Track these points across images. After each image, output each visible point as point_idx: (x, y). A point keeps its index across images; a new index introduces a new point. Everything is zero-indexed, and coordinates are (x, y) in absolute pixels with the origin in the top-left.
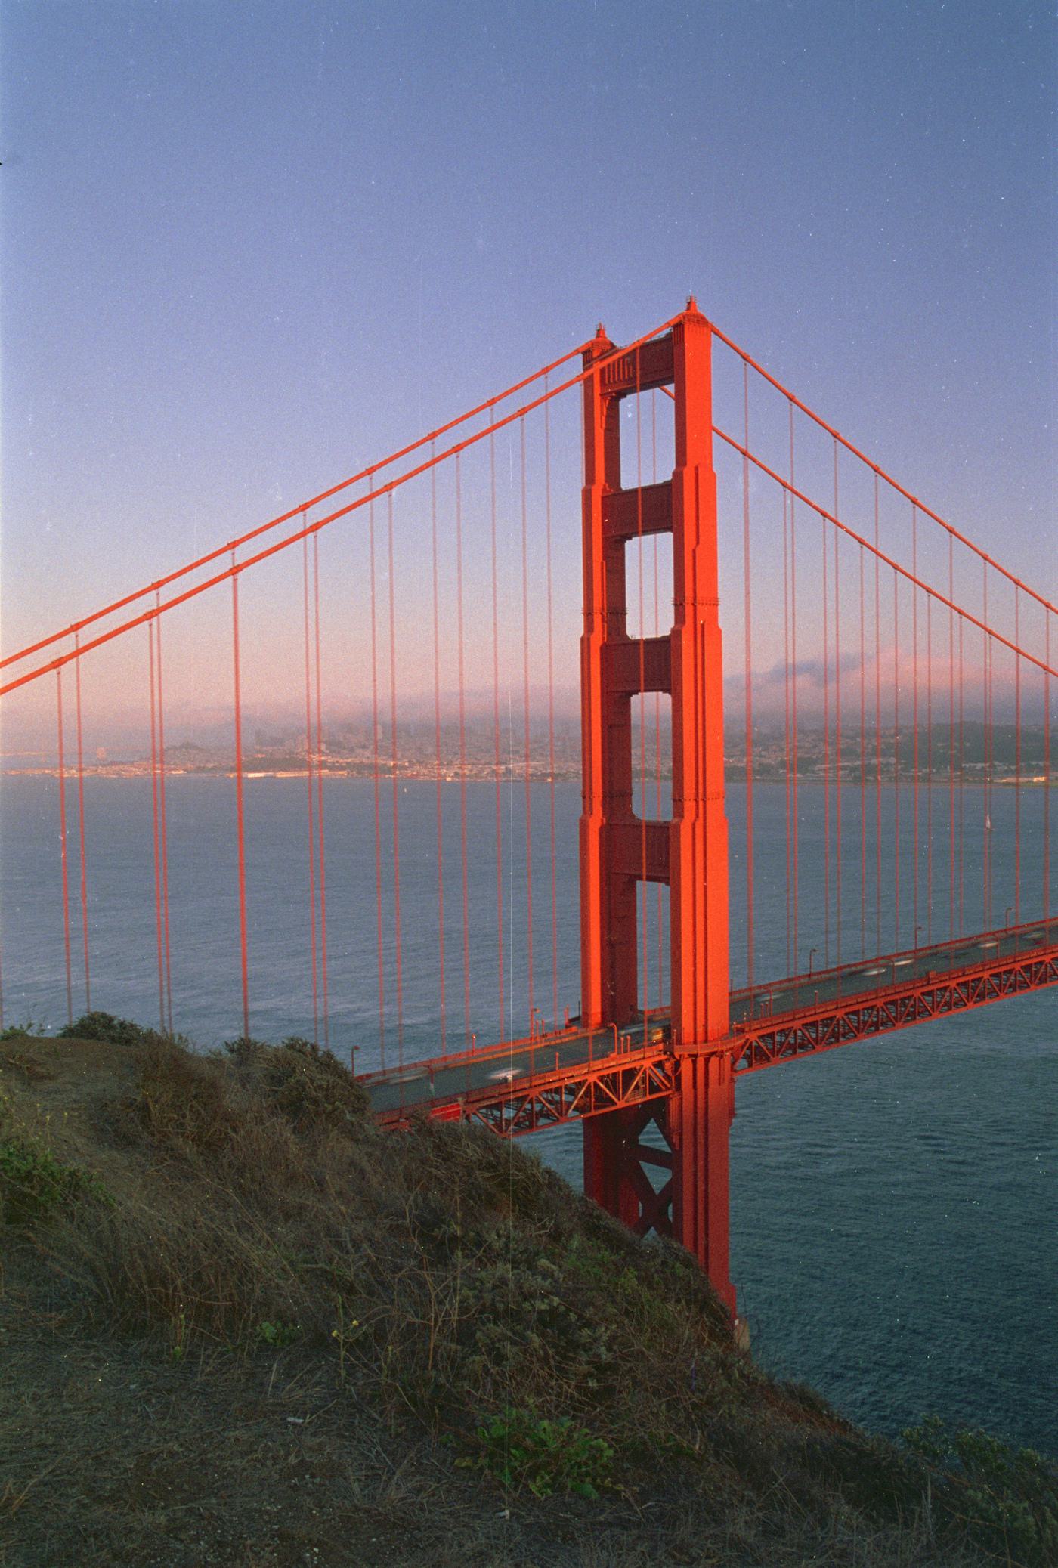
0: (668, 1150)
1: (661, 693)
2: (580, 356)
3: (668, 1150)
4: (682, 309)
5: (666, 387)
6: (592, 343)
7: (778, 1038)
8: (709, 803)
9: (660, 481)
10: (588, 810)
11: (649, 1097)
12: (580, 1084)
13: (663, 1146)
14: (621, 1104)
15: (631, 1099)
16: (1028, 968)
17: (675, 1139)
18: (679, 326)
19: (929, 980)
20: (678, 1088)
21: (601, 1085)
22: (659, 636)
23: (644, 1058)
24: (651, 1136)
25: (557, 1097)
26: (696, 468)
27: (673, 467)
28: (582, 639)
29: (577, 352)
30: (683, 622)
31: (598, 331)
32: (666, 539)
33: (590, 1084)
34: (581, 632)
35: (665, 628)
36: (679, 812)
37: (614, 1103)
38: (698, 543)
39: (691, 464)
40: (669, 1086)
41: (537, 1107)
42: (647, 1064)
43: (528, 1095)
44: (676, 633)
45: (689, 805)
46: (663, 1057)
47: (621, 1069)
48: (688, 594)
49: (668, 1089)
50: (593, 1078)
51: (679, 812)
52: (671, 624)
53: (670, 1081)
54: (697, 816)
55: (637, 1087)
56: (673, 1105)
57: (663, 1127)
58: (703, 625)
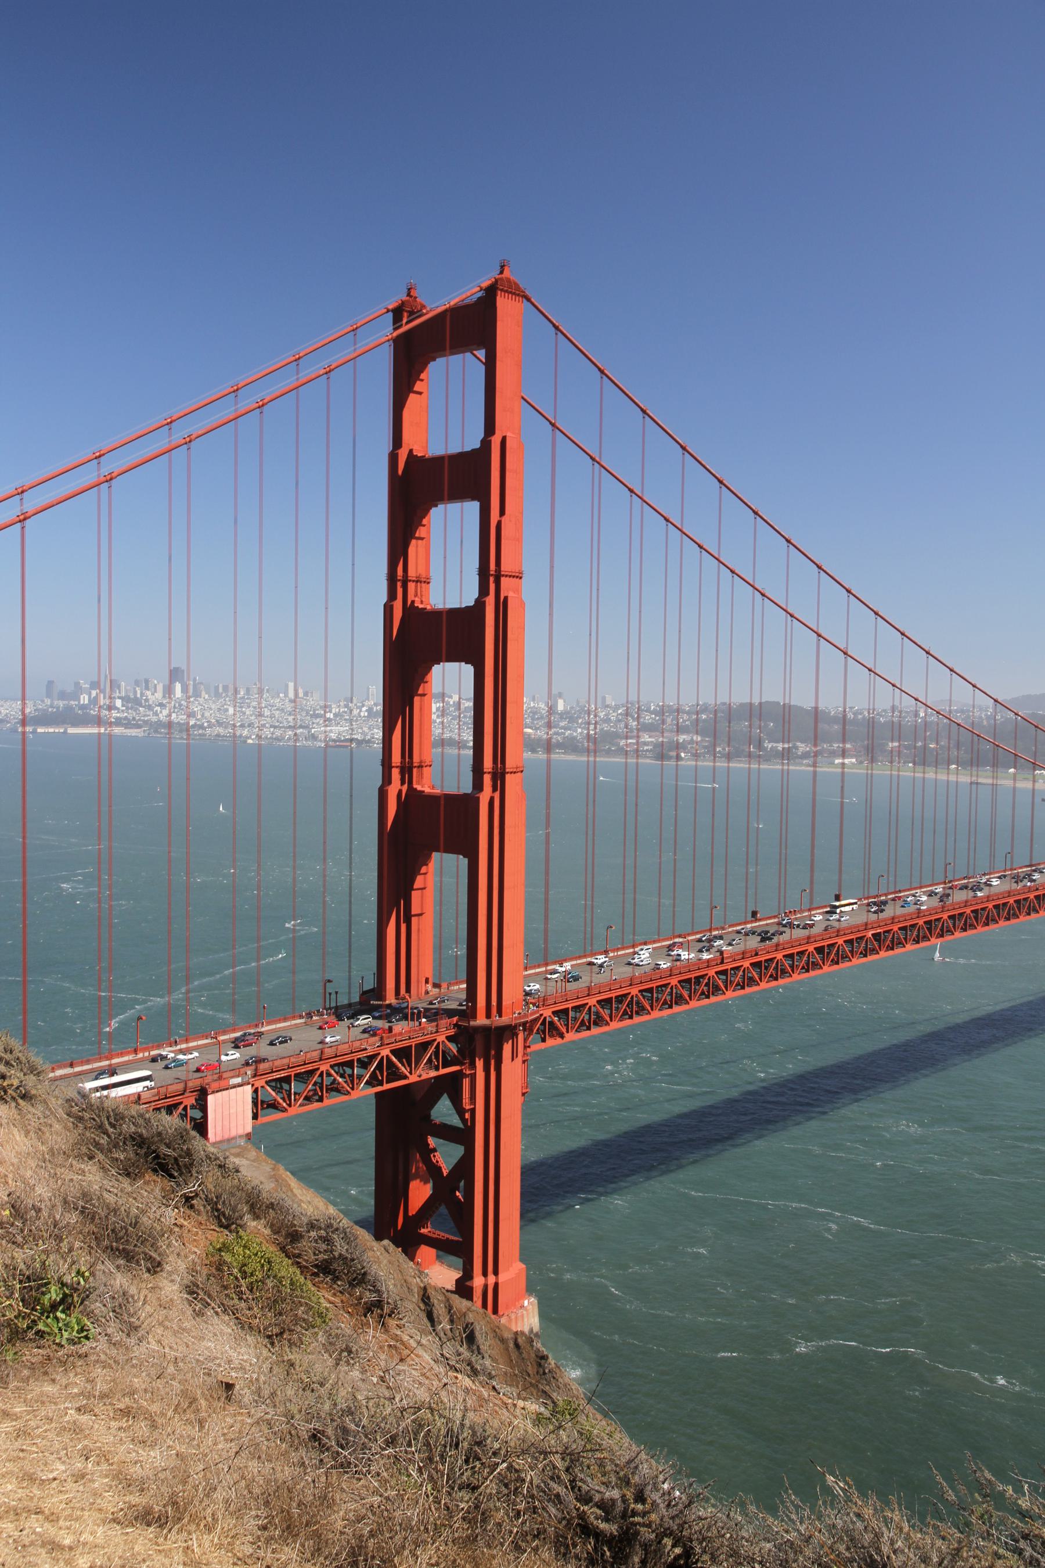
0: (461, 1126)
1: (463, 664)
2: (390, 315)
3: (461, 1126)
4: (494, 274)
5: (475, 352)
6: (403, 303)
7: (571, 1014)
8: (508, 776)
9: (468, 449)
10: (387, 779)
11: (443, 1071)
12: (372, 1058)
14: (413, 1079)
15: (422, 1073)
16: (820, 950)
18: (491, 292)
19: (723, 959)
21: (394, 1059)
22: (463, 606)
23: (437, 1032)
24: (443, 1111)
25: (348, 1071)
26: (504, 442)
27: (481, 435)
28: (385, 605)
30: (487, 594)
31: (409, 289)
32: (473, 507)
33: (383, 1057)
34: (384, 599)
35: (469, 599)
36: (478, 785)
37: (405, 1077)
38: (502, 512)
41: (327, 1081)
42: (441, 1038)
44: (480, 604)
45: (487, 779)
47: (413, 1043)
50: (385, 1052)
51: (478, 785)
52: (476, 595)
54: (494, 790)
55: (430, 1061)
57: (456, 1102)
58: (506, 598)
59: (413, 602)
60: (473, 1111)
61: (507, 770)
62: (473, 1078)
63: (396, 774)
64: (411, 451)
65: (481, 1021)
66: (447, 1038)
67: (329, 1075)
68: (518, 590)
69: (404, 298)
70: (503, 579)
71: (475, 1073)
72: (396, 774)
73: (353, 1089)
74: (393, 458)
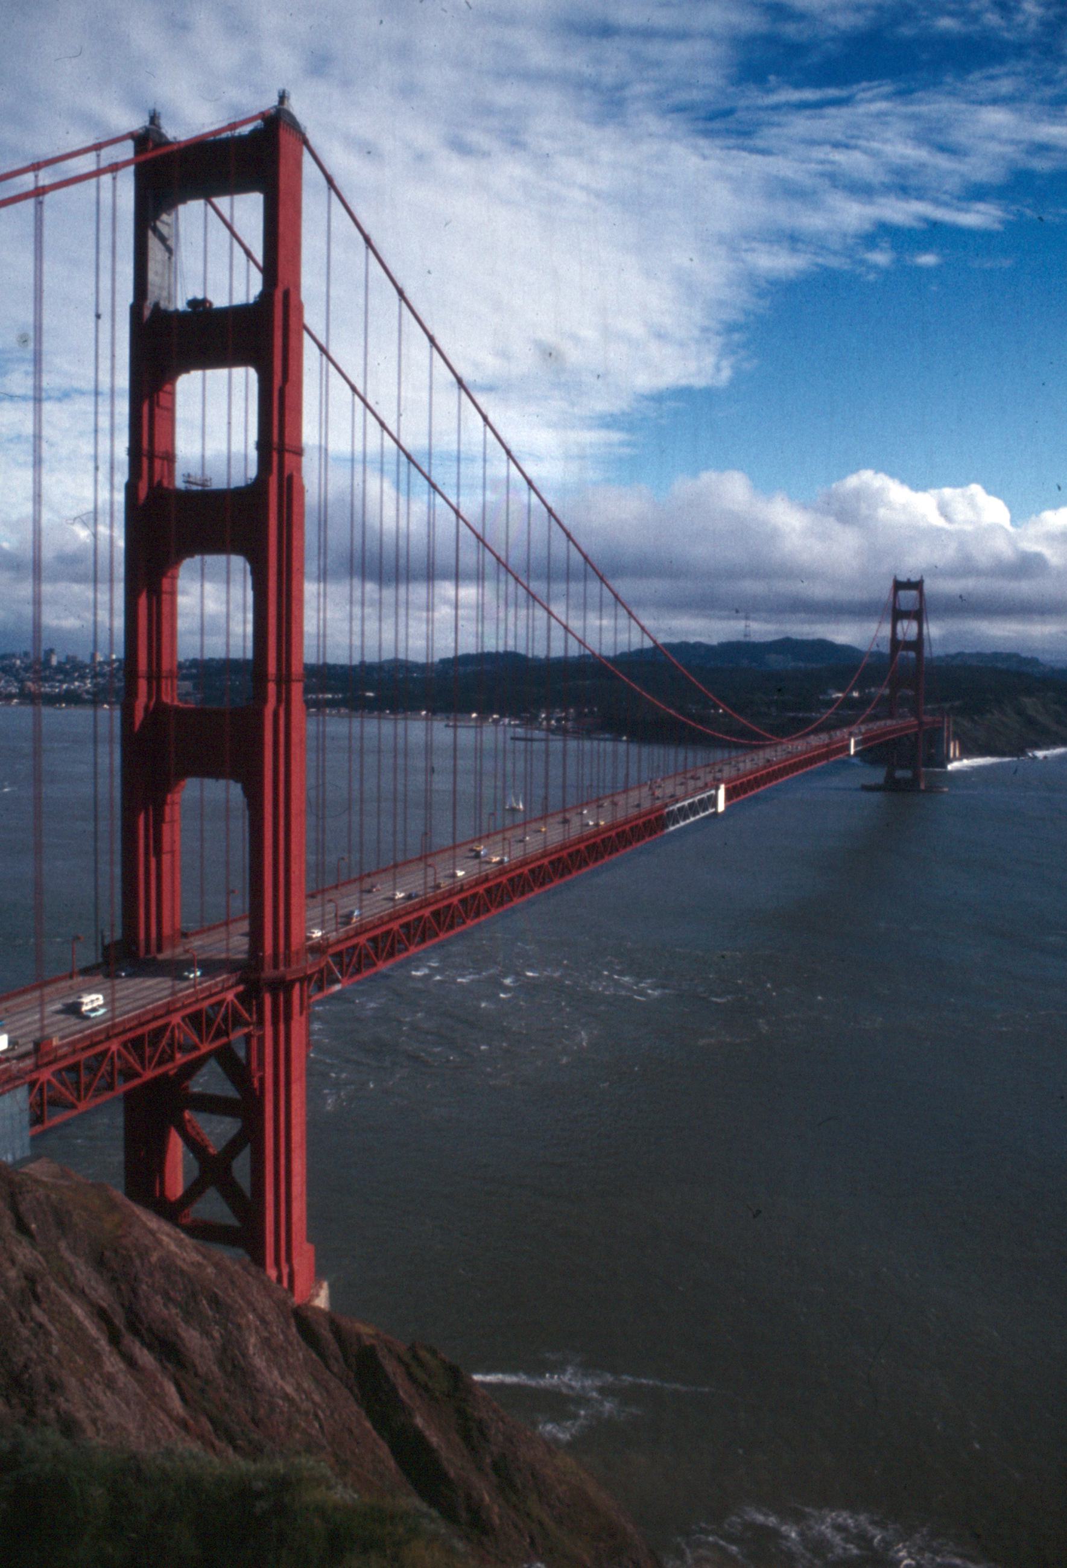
6: (147, 131)
7: (346, 960)
13: (229, 1091)
17: (256, 1084)
20: (261, 1022)
29: (132, 136)
36: (260, 697)
39: (280, 285)
40: (249, 1019)
42: (230, 996)
43: (109, 1049)
45: (272, 687)
46: (241, 988)
48: (276, 438)
49: (247, 1024)
53: (249, 1011)
54: (279, 701)
56: (254, 1042)
59: (160, 483)
60: (262, 1080)
61: (294, 677)
62: (261, 1040)
63: (143, 684)
64: (157, 305)
65: (268, 973)
66: (237, 996)
67: (120, 1055)
68: (299, 468)
69: (147, 124)
70: (287, 455)
71: (264, 1035)
72: (143, 684)
73: (144, 1068)
74: (136, 310)
